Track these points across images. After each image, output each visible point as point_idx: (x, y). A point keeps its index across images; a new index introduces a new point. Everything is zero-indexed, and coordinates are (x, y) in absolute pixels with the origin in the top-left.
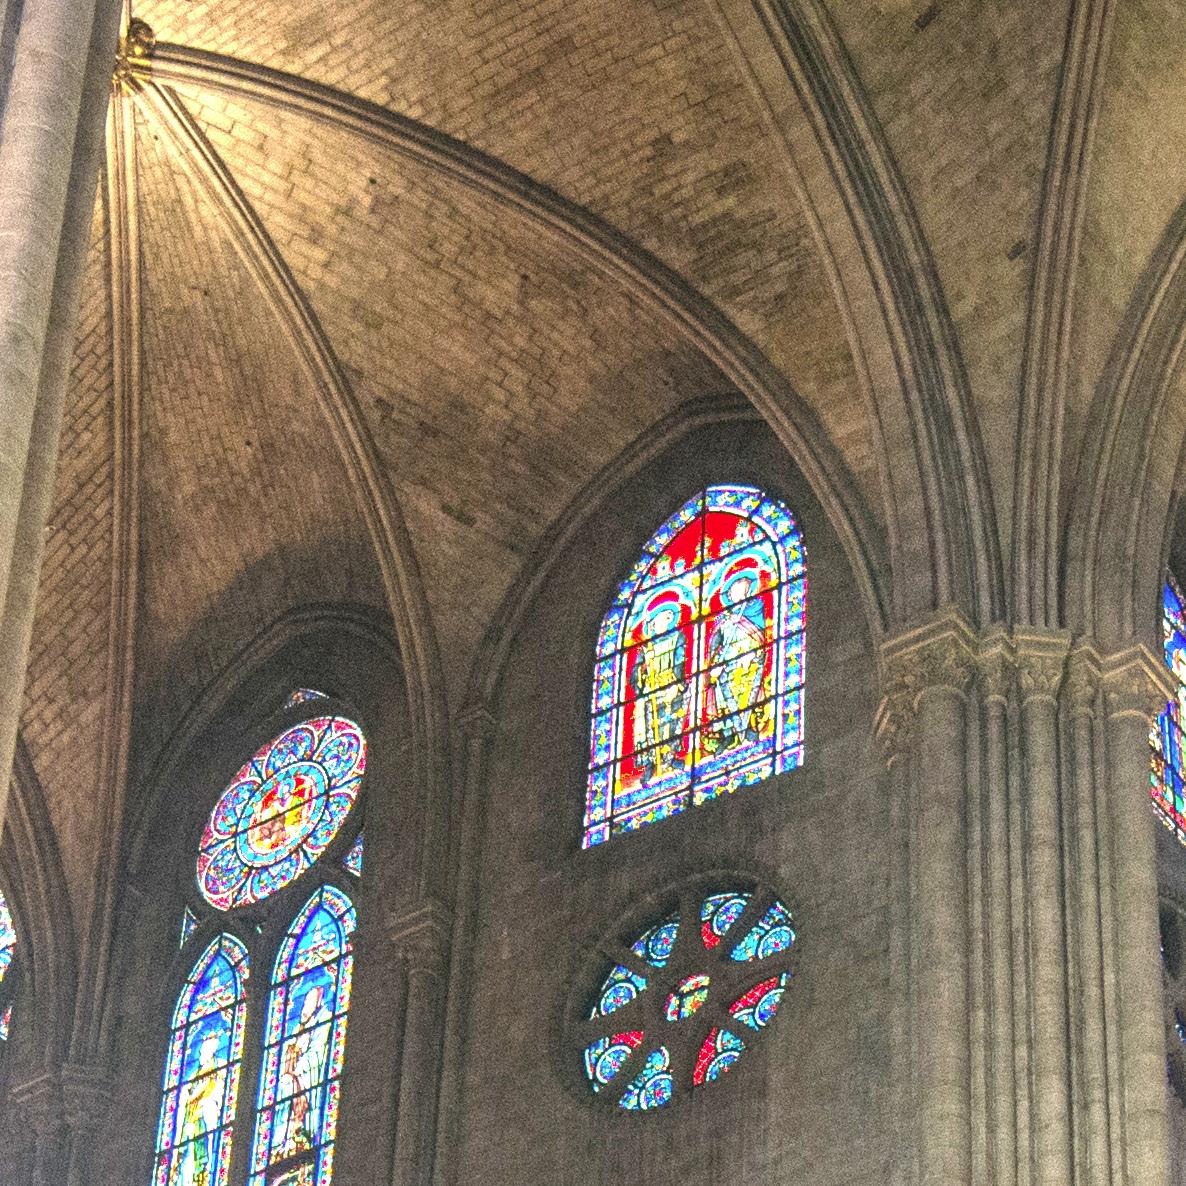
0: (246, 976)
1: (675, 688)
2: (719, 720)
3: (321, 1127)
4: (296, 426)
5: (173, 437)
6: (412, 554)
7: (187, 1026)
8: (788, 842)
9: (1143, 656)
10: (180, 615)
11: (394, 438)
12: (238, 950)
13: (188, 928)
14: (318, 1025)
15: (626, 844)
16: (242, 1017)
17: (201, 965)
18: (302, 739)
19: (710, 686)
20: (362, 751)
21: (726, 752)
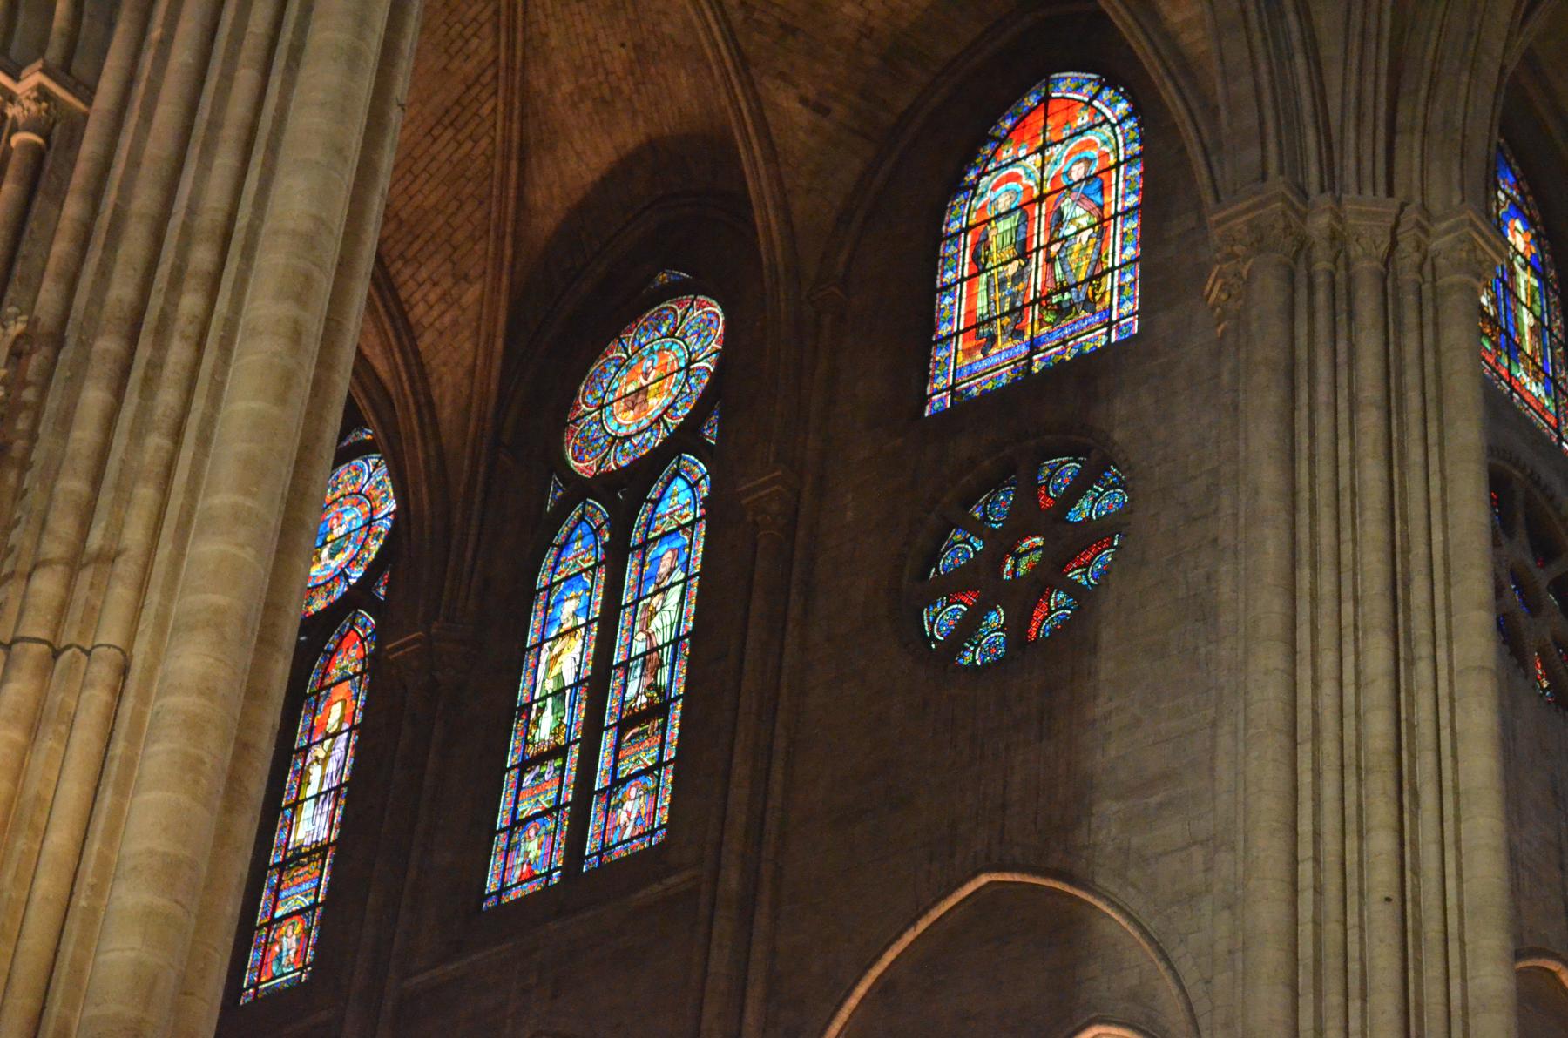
0: (607, 538)
1: (1016, 263)
2: (1056, 293)
3: (671, 683)
4: (667, 28)
5: (553, 42)
6: (772, 145)
7: (550, 587)
8: (1120, 408)
9: (1472, 224)
10: (557, 206)
11: (757, 37)
12: (599, 512)
13: (555, 494)
14: (673, 585)
15: (967, 409)
16: (602, 575)
17: (565, 529)
18: (667, 317)
19: (1050, 260)
20: (721, 328)
21: (1064, 323)
